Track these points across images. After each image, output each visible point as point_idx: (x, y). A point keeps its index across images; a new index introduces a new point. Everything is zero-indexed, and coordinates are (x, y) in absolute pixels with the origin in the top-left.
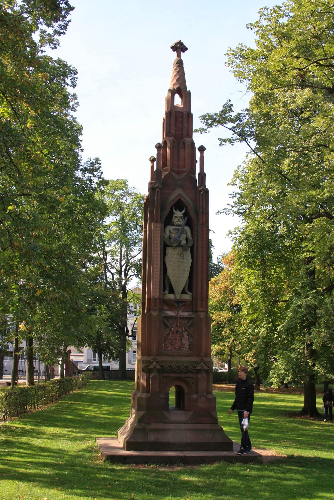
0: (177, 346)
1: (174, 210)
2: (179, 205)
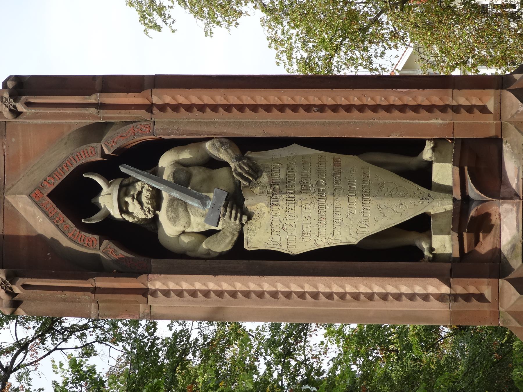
1: (95, 219)
2: (73, 197)
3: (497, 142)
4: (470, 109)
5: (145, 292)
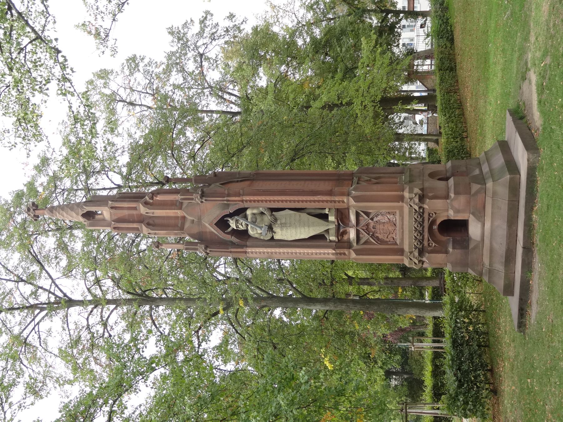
0: (391, 228)
1: (230, 230)
3: (348, 209)
4: (339, 202)
5: (246, 252)
